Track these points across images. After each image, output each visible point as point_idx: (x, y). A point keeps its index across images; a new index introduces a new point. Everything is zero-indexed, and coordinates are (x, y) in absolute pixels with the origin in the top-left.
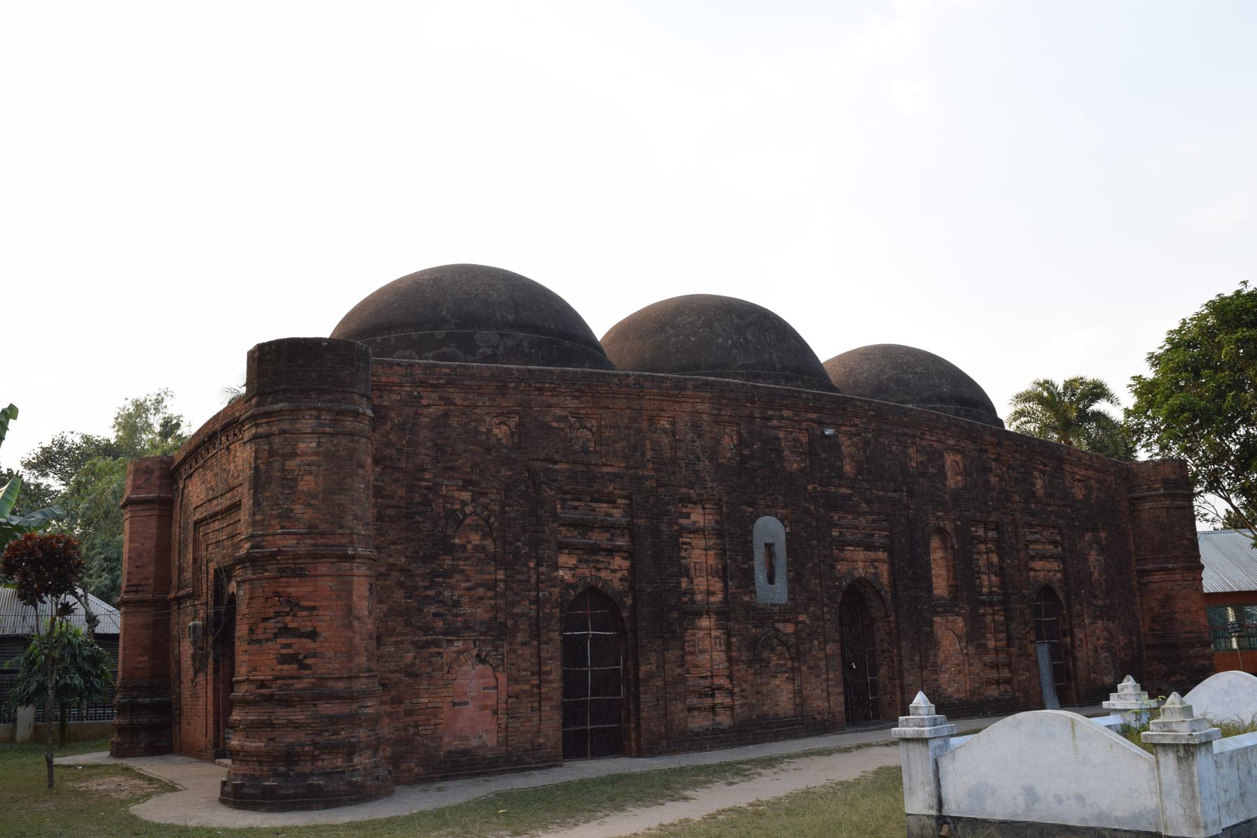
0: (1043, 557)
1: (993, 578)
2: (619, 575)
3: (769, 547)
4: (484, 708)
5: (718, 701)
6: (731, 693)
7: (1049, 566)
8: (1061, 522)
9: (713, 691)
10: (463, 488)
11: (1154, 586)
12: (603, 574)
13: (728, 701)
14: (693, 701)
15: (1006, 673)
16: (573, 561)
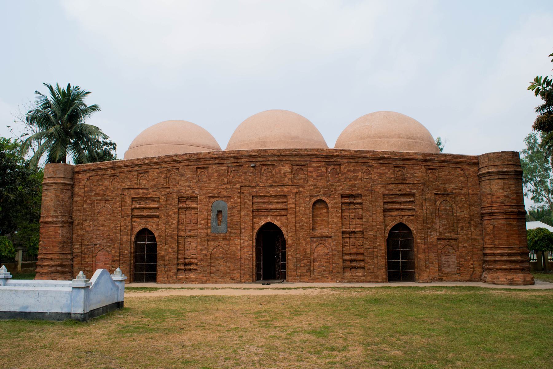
0: (397, 210)
1: (358, 220)
2: (156, 223)
3: (219, 212)
4: (105, 264)
5: (191, 267)
6: (196, 264)
7: (403, 213)
8: (413, 191)
9: (191, 264)
10: (101, 200)
11: (485, 222)
12: (149, 224)
13: (195, 267)
14: (182, 267)
15: (362, 265)
16: (138, 220)
